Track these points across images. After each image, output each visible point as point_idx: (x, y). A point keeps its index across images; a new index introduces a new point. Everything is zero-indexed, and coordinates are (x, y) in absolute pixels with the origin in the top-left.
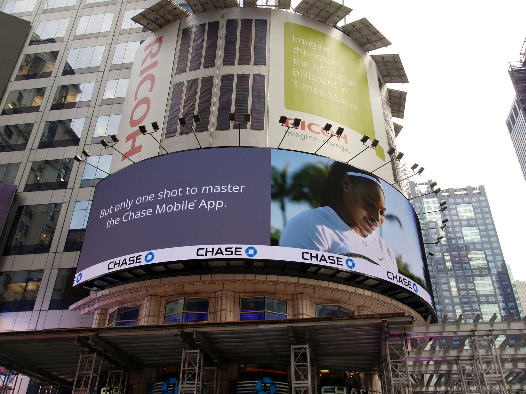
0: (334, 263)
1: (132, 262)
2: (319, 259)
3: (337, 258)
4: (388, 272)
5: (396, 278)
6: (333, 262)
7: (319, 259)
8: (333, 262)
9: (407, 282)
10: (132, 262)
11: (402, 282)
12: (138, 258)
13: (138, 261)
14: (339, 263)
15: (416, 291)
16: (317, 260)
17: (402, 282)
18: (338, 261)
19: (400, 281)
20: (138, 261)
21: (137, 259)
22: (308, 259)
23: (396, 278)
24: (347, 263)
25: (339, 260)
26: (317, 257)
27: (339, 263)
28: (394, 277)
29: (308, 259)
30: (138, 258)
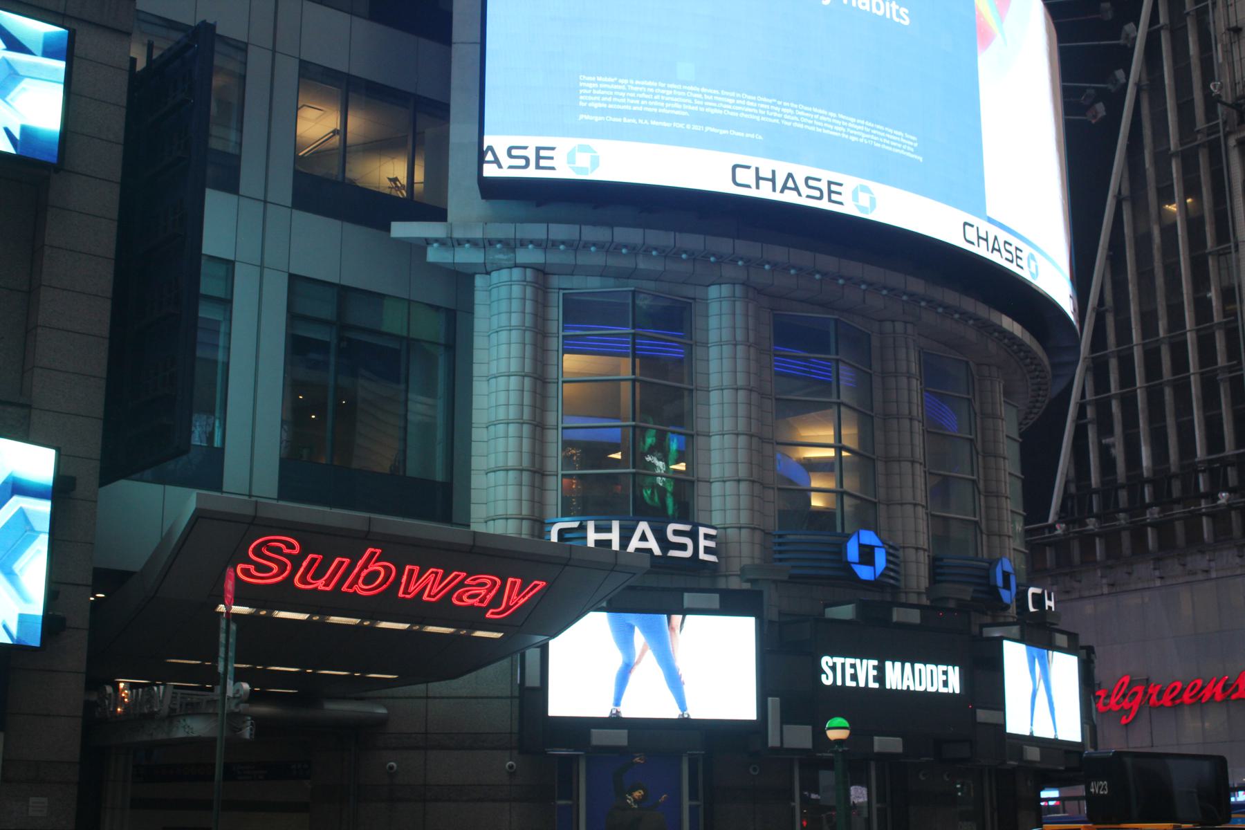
0: (821, 198)
2: (779, 186)
3: (830, 183)
4: (965, 224)
5: (986, 240)
6: (817, 194)
7: (779, 186)
8: (817, 194)
9: (1012, 249)
11: (999, 251)
14: (834, 197)
15: (1035, 275)
16: (774, 190)
17: (999, 251)
18: (830, 192)
19: (994, 249)
22: (748, 186)
23: (986, 240)
24: (855, 197)
25: (833, 188)
26: (773, 180)
27: (834, 197)
28: (979, 238)
29: (748, 186)
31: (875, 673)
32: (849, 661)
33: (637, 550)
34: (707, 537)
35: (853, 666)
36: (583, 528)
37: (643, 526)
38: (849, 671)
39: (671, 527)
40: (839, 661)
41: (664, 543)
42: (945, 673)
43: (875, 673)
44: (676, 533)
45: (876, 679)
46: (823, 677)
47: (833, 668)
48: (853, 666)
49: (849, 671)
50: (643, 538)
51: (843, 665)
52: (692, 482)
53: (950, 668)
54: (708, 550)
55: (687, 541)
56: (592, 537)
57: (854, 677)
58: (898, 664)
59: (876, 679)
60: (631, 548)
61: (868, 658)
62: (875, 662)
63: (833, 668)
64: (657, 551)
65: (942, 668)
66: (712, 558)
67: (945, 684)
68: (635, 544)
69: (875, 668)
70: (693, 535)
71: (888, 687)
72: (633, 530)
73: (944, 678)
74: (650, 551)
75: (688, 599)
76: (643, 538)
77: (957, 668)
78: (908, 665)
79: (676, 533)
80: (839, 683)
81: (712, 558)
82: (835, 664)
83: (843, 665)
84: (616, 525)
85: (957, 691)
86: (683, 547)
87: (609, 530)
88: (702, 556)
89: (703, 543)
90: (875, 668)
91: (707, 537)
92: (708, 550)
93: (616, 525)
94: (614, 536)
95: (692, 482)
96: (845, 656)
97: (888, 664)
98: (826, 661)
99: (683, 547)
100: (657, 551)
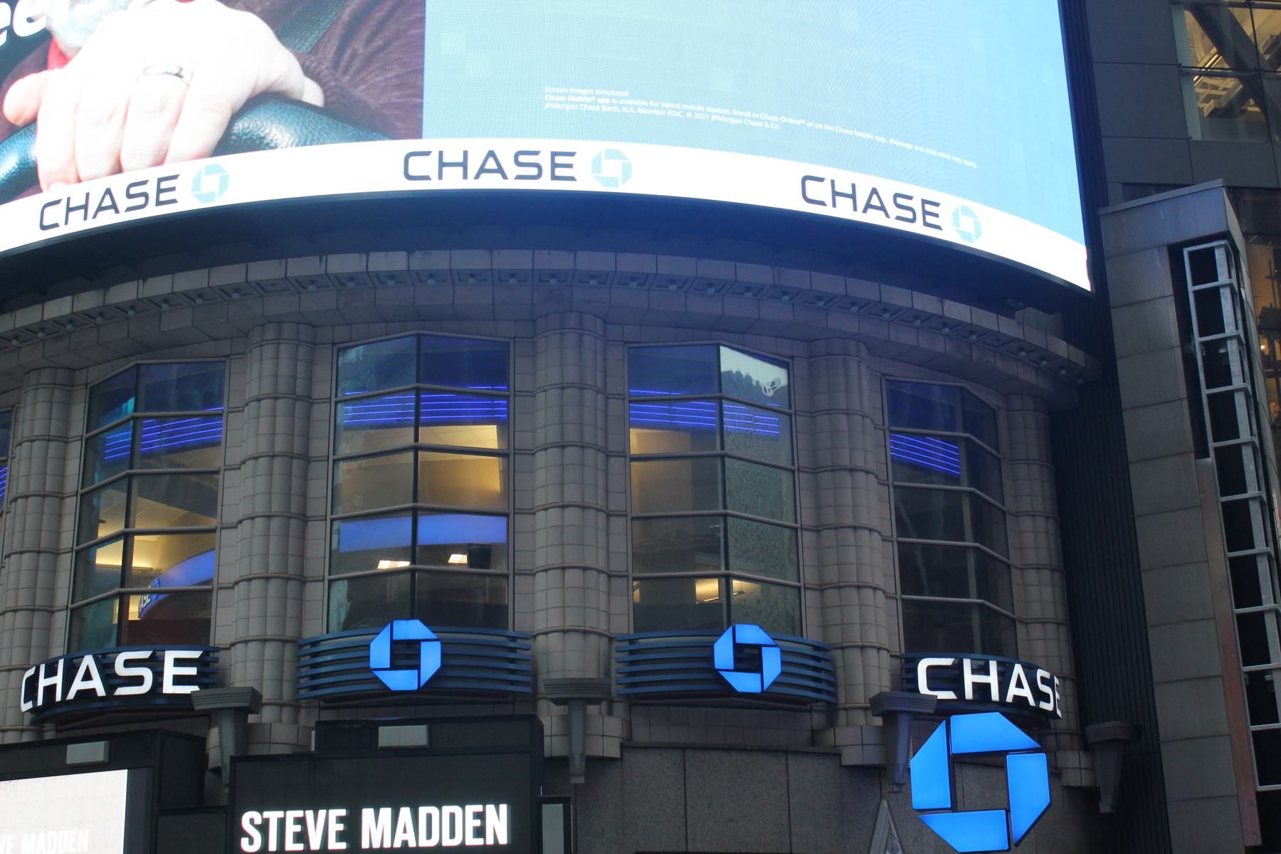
1: (141, 201)
10: (141, 201)
12: (164, 185)
13: (163, 197)
20: (163, 197)
21: (160, 191)
30: (164, 185)
31: (341, 827)
32: (292, 815)
33: (80, 693)
34: (178, 662)
35: (301, 821)
37: (88, 661)
38: (292, 828)
40: (273, 816)
41: (111, 680)
42: (481, 816)
43: (341, 827)
44: (128, 663)
45: (341, 836)
46: (244, 842)
47: (264, 828)
48: (301, 821)
49: (292, 828)
50: (87, 677)
51: (282, 823)
52: (211, 591)
53: (490, 808)
54: (178, 680)
56: (43, 682)
57: (302, 837)
58: (386, 812)
59: (341, 836)
60: (71, 695)
61: (328, 807)
62: (343, 812)
63: (264, 828)
64: (101, 692)
65: (472, 809)
67: (480, 832)
68: (78, 685)
69: (340, 820)
71: (365, 845)
73: (478, 823)
74: (94, 690)
75: (76, 753)
76: (87, 677)
77: (503, 808)
78: (405, 812)
79: (128, 663)
80: (273, 847)
82: (266, 822)
83: (282, 823)
85: (503, 840)
86: (139, 681)
88: (169, 688)
89: (170, 671)
90: (340, 820)
91: (178, 662)
92: (178, 680)
94: (58, 680)
95: (211, 591)
96: (285, 809)
97: (367, 813)
98: (250, 819)
99: (139, 681)
100: (101, 692)
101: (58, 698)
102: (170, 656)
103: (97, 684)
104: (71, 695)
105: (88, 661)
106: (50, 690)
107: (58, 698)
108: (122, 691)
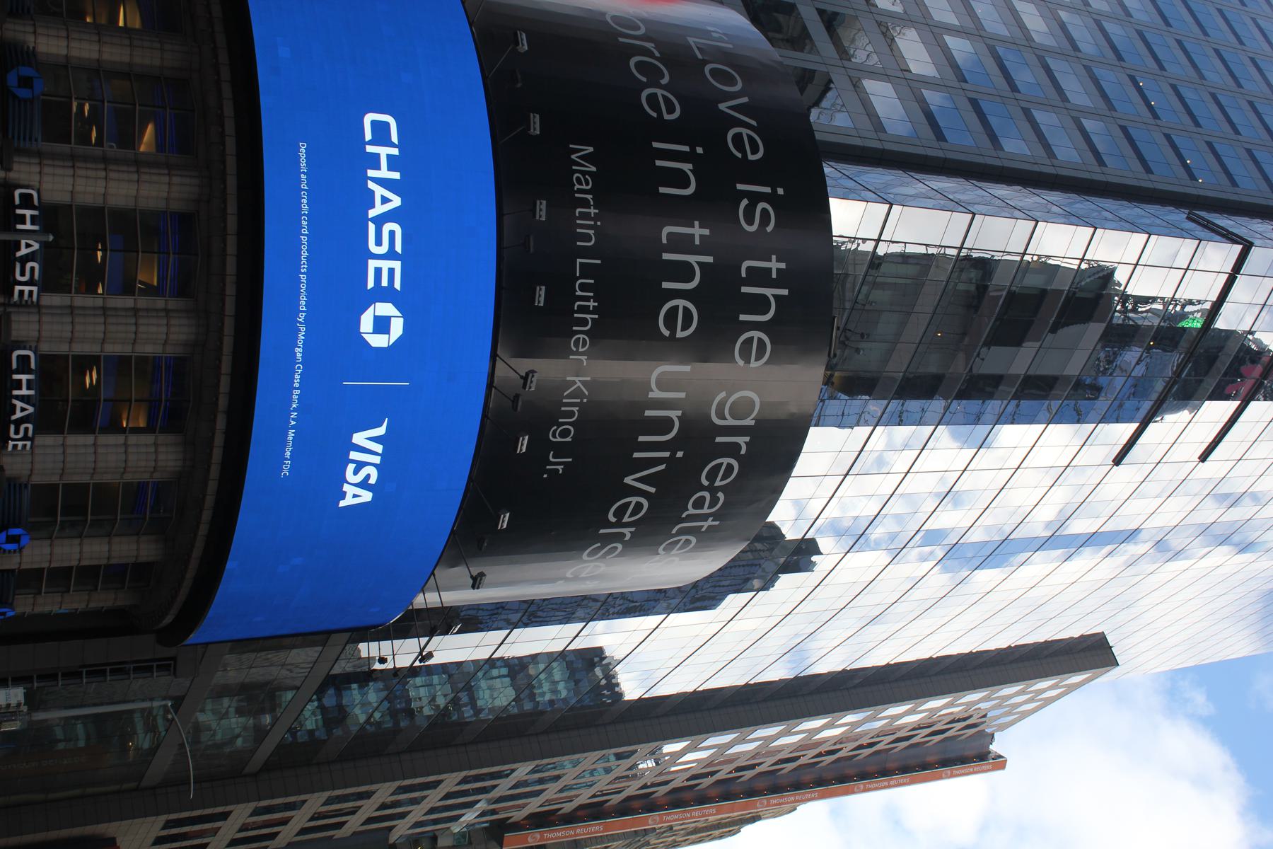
36: (29, 372)
37: (31, 409)
39: (30, 426)
54: (15, 446)
55: (21, 435)
60: (15, 402)
66: (10, 448)
68: (19, 404)
70: (25, 438)
72: (28, 403)
76: (23, 410)
81: (10, 448)
84: (31, 392)
86: (17, 432)
87: (29, 388)
88: (11, 443)
91: (25, 446)
92: (15, 446)
93: (31, 392)
94: (24, 392)
99: (17, 432)
101: (16, 392)
102: (29, 443)
103: (19, 415)
104: (15, 402)
105: (31, 409)
106: (18, 385)
107: (16, 392)
108: (12, 428)
